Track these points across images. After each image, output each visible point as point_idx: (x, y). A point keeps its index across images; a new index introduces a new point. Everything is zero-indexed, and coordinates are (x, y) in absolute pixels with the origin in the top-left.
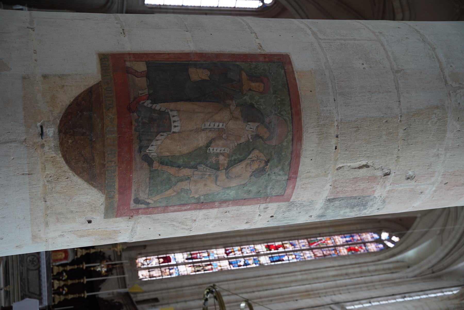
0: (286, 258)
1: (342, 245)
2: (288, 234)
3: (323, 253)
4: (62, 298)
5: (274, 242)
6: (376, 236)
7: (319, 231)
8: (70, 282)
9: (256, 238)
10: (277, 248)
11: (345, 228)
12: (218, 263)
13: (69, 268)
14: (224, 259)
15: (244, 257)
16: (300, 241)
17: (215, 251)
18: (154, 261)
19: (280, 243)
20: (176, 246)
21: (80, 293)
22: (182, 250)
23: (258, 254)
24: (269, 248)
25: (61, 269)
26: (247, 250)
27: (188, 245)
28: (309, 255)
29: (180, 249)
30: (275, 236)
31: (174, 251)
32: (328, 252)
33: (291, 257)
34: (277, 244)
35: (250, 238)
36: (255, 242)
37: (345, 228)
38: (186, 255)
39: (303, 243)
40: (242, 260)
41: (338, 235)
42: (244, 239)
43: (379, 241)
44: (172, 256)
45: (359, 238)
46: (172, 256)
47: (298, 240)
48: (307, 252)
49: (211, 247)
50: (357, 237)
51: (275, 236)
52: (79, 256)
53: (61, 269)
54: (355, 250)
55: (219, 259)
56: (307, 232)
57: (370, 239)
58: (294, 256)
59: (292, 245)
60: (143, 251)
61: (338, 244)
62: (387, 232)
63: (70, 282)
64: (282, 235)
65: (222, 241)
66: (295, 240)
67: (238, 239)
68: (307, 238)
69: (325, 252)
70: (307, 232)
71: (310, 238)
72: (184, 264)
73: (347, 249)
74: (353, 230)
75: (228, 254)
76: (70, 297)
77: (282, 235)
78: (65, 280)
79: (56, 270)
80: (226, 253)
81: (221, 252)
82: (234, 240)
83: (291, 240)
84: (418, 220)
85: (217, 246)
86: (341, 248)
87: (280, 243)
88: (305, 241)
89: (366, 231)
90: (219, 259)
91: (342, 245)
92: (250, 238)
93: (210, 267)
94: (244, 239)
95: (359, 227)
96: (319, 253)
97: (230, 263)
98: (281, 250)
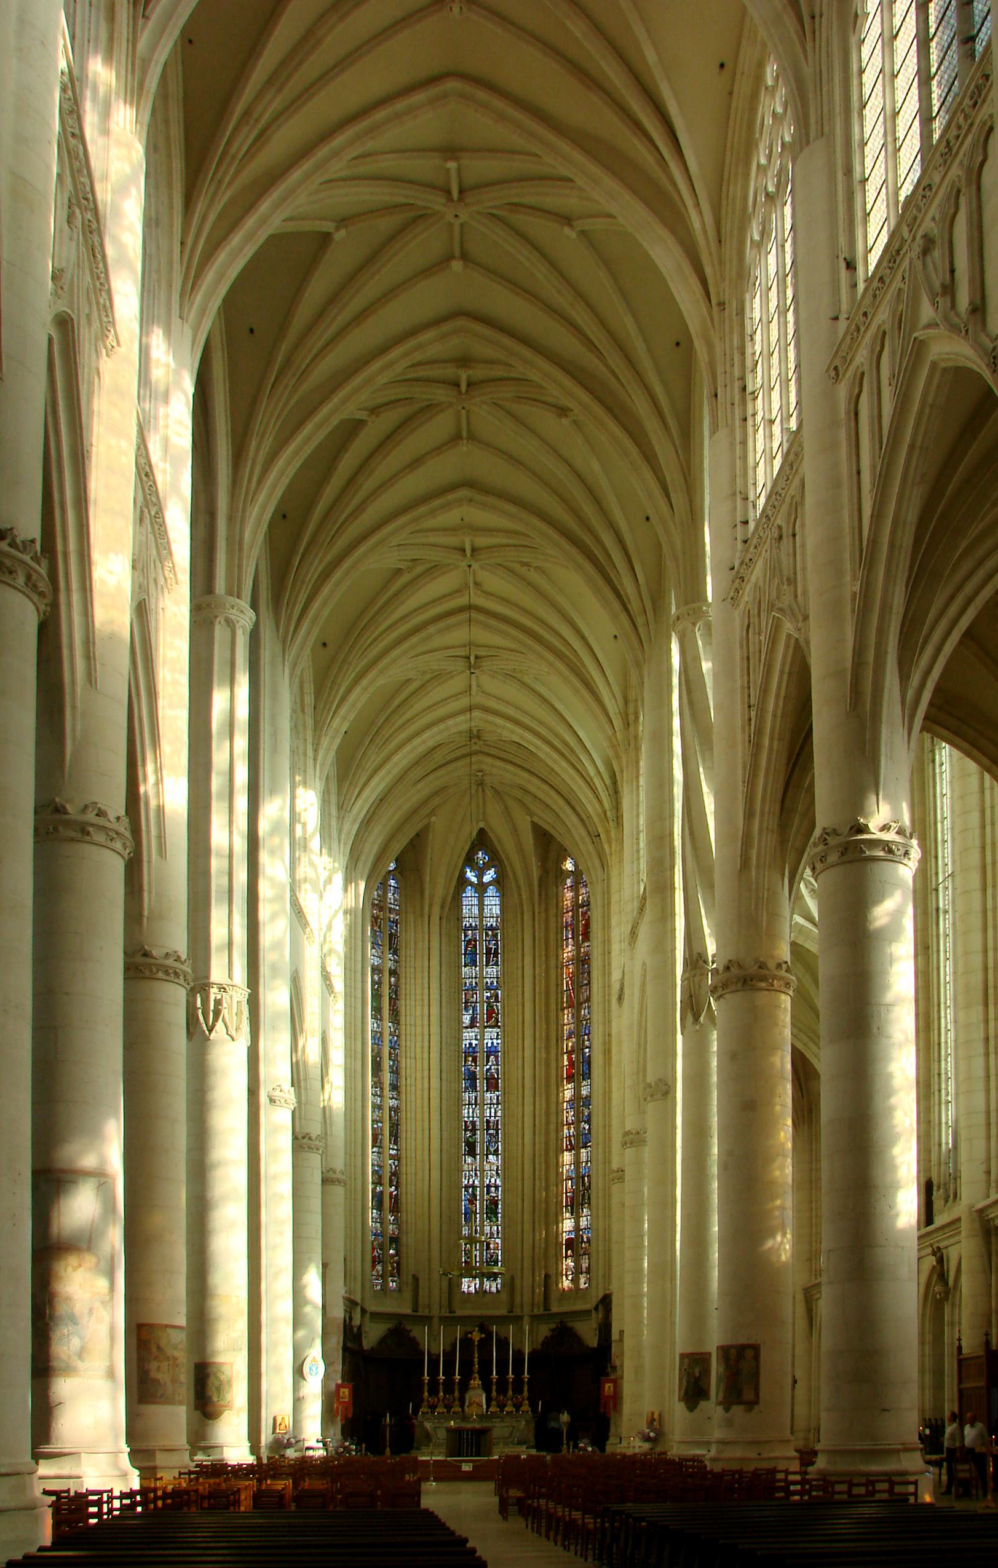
2: (553, 1042)
3: (586, 985)
7: (553, 988)
8: (510, 1393)
9: (553, 1099)
10: (571, 1063)
13: (494, 1394)
14: (577, 1157)
19: (565, 1057)
27: (552, 1210)
30: (553, 1064)
34: (566, 1063)
42: (553, 1119)
43: (577, 874)
51: (553, 1064)
53: (494, 1403)
56: (553, 1007)
63: (510, 1393)
67: (552, 1127)
71: (562, 1002)
74: (557, 922)
80: (570, 1151)
82: (553, 1134)
84: (536, 819)
89: (559, 898)
95: (553, 911)
97: (585, 1147)
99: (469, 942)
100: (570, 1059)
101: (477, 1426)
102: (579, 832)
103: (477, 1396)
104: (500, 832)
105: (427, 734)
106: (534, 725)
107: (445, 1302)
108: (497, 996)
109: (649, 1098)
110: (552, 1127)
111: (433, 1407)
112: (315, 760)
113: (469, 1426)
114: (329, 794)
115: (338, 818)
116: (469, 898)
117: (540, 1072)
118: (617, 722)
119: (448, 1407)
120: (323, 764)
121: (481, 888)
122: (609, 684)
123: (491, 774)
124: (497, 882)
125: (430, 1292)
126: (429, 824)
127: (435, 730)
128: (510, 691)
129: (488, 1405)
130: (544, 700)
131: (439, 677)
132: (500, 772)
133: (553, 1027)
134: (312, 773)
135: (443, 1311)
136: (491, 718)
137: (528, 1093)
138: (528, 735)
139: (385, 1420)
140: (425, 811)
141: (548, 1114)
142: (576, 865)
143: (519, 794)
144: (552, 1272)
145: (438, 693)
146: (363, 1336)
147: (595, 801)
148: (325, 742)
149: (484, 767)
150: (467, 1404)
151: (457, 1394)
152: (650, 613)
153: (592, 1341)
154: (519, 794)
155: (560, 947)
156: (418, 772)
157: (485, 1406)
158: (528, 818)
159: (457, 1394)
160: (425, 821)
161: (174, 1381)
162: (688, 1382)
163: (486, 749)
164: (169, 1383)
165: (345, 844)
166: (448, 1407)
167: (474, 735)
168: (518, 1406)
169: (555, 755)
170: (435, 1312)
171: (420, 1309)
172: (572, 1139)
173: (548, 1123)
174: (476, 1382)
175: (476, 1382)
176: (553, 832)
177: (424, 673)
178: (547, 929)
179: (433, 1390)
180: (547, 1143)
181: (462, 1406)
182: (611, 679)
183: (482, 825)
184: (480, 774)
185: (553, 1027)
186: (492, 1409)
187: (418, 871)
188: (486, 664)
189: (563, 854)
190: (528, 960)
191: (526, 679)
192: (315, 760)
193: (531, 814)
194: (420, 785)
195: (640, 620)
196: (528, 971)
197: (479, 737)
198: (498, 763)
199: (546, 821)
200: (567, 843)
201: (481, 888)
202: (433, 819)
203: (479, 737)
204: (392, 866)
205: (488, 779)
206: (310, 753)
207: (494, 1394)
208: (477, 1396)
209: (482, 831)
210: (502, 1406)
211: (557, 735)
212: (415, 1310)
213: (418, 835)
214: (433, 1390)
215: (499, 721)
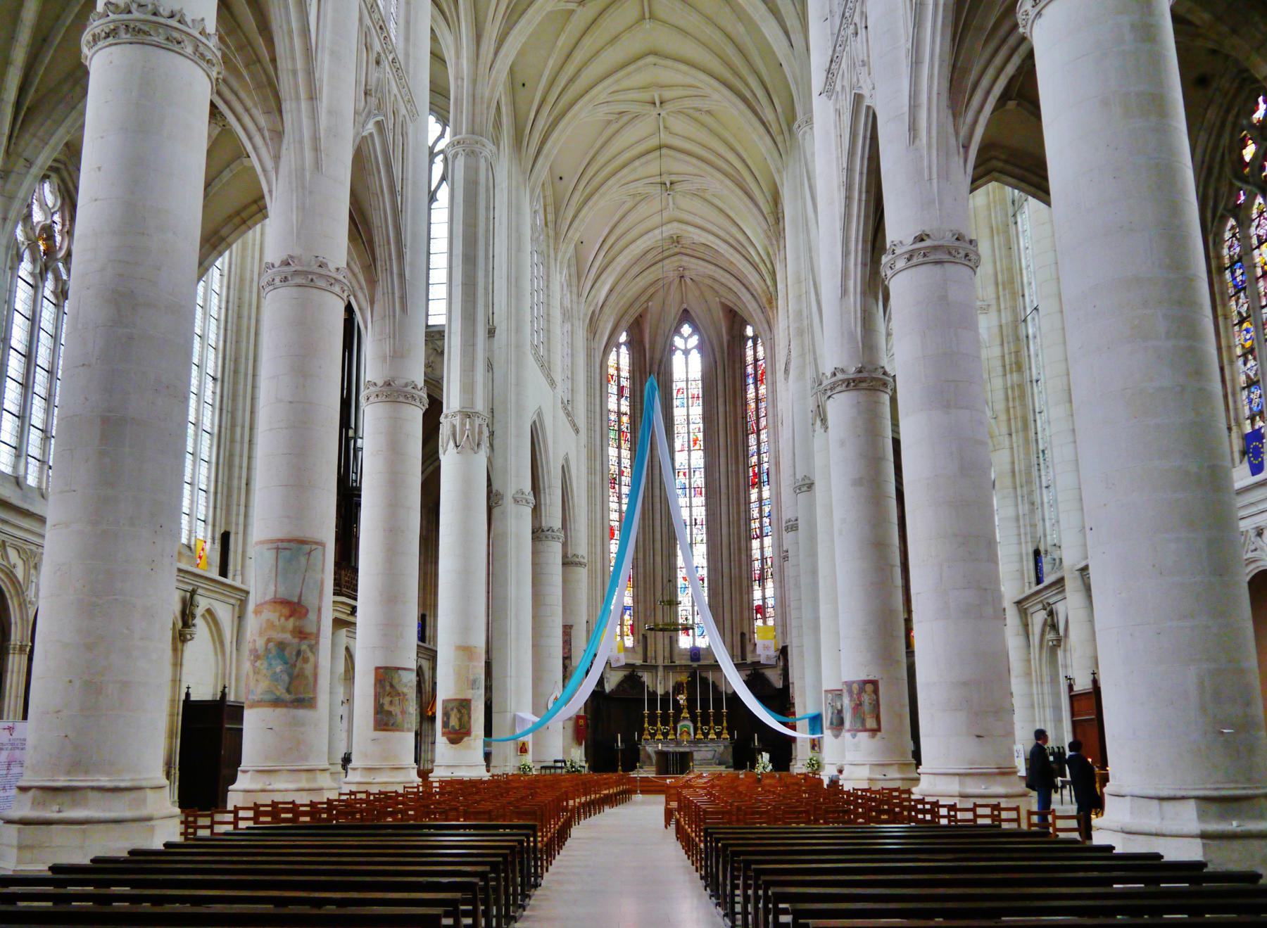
0: (765, 466)
1: (757, 389)
2: (741, 459)
4: (725, 731)
5: (748, 477)
6: (750, 343)
7: (739, 420)
8: (712, 724)
9: (742, 501)
10: (755, 475)
11: (738, 384)
12: (766, 550)
13: (699, 725)
15: (761, 517)
16: (750, 444)
17: (754, 552)
18: (759, 623)
20: (745, 597)
21: (709, 716)
22: (750, 590)
23: (760, 499)
24: (753, 485)
25: (699, 732)
26: (755, 514)
27: (745, 583)
28: (765, 435)
29: (748, 594)
30: (741, 475)
31: (751, 600)
32: (763, 410)
33: (766, 460)
34: (751, 474)
35: (742, 508)
36: (748, 502)
37: (738, 384)
38: (756, 587)
39: (752, 439)
40: (765, 519)
41: (746, 392)
42: (742, 515)
44: (756, 603)
45: (751, 366)
46: (756, 603)
47: (748, 446)
48: (762, 437)
49: (749, 556)
50: (750, 370)
51: (741, 475)
52: (688, 715)
53: (699, 732)
54: (762, 374)
55: (762, 548)
56: (740, 434)
57: (752, 352)
58: (764, 455)
59: (753, 455)
60: (747, 636)
61: (754, 394)
62: (746, 328)
63: (712, 724)
64: (741, 467)
65: (743, 543)
66: (748, 451)
67: (742, 522)
68: (747, 435)
69: (763, 414)
70: (740, 434)
71: (747, 430)
72: (764, 589)
73: (761, 384)
75: (758, 537)
76: (725, 724)
77: (741, 467)
78: (723, 728)
79: (699, 736)
81: (756, 544)
82: (743, 528)
83: (748, 455)
84: (723, 300)
85: (749, 549)
86: (760, 392)
87: (751, 469)
88: (750, 436)
89: (743, 356)
90: (762, 548)
91: (757, 389)
92: (742, 508)
93: (769, 561)
94: (742, 515)
95: (737, 366)
96: (763, 422)
98: (756, 469)
99: (679, 390)
100: (754, 471)
101: (687, 750)
102: (752, 306)
103: (686, 724)
104: (696, 309)
105: (639, 242)
106: (714, 229)
107: (667, 654)
108: (699, 429)
109: (798, 491)
110: (742, 522)
111: (653, 735)
112: (556, 260)
113: (682, 750)
114: (571, 286)
115: (578, 303)
116: (678, 360)
117: (732, 482)
118: (771, 219)
119: (665, 735)
120: (561, 263)
121: (686, 352)
122: (763, 192)
123: (689, 269)
124: (700, 347)
125: (655, 647)
126: (647, 307)
127: (645, 238)
128: (697, 205)
129: (695, 734)
130: (721, 210)
131: (646, 197)
132: (697, 268)
133: (740, 448)
134: (554, 269)
135: (666, 661)
136: (684, 227)
137: (724, 497)
138: (711, 238)
139: (617, 746)
140: (643, 299)
141: (738, 513)
142: (754, 331)
143: (708, 281)
144: (746, 630)
145: (643, 209)
146: (605, 680)
147: (762, 284)
148: (563, 247)
149: (683, 264)
150: (679, 732)
151: (671, 724)
152: (786, 133)
153: (779, 684)
154: (710, 282)
155: (745, 391)
156: (636, 270)
157: (692, 735)
158: (717, 299)
159: (671, 724)
160: (645, 306)
161: (403, 712)
162: (833, 713)
163: (683, 251)
164: (399, 713)
165: (584, 321)
166: (665, 735)
167: (676, 240)
168: (719, 734)
169: (731, 250)
170: (660, 662)
171: (649, 661)
172: (758, 530)
173: (739, 520)
174: (685, 714)
175: (685, 714)
176: (735, 308)
177: (634, 195)
178: (734, 378)
179: (653, 722)
180: (739, 534)
181: (675, 734)
182: (762, 184)
183: (685, 306)
184: (681, 269)
185: (740, 448)
186: (697, 737)
187: (641, 342)
188: (678, 187)
189: (744, 323)
190: (721, 400)
191: (709, 197)
192: (556, 260)
193: (720, 296)
194: (638, 279)
195: (779, 139)
196: (721, 409)
197: (678, 242)
198: (693, 260)
199: (730, 300)
200: (746, 317)
201: (686, 352)
202: (650, 304)
203: (678, 242)
204: (623, 338)
205: (687, 273)
206: (552, 255)
207: (699, 725)
208: (686, 724)
209: (686, 311)
210: (706, 735)
211: (731, 236)
212: (645, 661)
213: (641, 316)
214: (653, 722)
215: (691, 229)
